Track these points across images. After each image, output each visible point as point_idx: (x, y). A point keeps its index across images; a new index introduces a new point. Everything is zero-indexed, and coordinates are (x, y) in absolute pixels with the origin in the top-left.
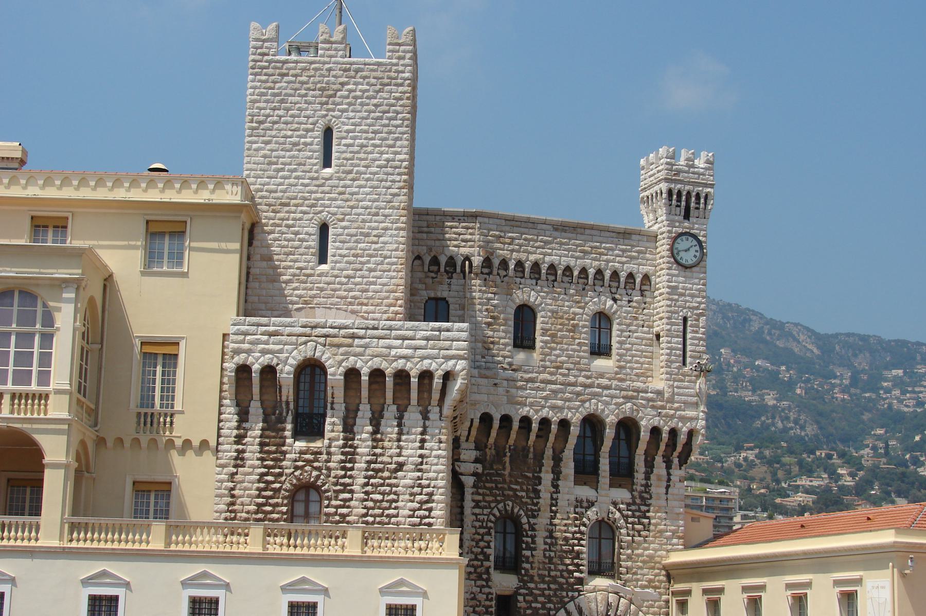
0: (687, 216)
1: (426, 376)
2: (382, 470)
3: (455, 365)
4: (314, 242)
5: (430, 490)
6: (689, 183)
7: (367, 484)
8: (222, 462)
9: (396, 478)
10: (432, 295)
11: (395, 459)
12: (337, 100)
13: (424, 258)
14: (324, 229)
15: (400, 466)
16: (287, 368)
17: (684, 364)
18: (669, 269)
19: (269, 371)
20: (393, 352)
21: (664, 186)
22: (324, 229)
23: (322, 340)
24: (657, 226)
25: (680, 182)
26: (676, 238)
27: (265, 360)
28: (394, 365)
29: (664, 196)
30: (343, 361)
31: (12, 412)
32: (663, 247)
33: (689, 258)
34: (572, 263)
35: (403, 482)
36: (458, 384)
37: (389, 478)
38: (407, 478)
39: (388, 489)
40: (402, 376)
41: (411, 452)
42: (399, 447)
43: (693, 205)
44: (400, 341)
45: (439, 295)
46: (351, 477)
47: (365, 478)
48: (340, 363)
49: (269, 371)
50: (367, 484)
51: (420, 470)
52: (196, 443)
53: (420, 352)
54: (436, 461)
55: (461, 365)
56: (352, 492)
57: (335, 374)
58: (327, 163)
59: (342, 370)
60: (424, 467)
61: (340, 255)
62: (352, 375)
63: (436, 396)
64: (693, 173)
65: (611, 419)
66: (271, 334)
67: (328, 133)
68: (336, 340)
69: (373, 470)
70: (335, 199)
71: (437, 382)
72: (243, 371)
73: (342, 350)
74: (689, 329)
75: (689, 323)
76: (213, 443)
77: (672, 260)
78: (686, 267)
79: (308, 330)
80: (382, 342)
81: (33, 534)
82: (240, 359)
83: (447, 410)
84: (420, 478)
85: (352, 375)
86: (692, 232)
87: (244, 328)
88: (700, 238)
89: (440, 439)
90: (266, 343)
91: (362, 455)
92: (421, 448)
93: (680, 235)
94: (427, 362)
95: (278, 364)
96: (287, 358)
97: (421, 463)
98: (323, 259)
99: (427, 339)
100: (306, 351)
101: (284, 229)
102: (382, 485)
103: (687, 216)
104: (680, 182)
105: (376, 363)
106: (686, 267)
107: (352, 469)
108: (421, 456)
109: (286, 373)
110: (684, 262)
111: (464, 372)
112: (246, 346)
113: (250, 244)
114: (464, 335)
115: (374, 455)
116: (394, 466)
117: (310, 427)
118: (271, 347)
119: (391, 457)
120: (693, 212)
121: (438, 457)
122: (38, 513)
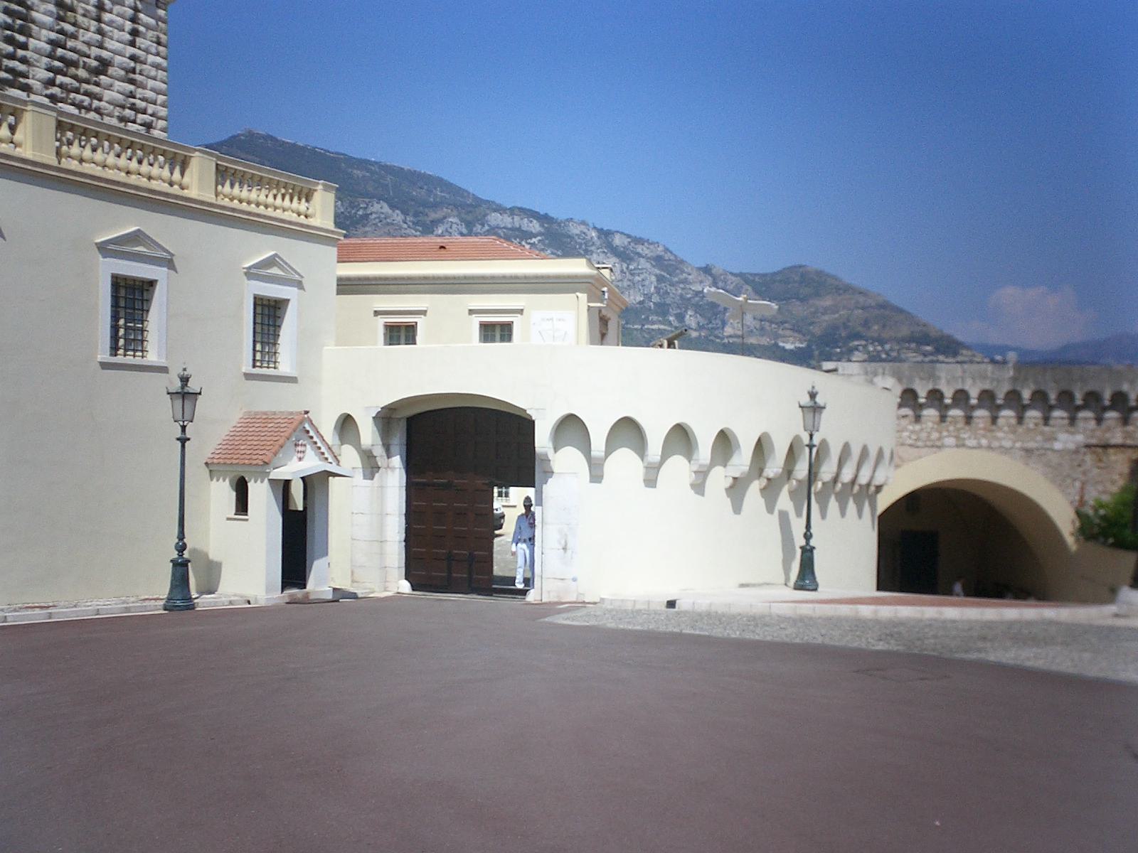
2: (74, 64)
5: (146, 118)
7: (51, 83)
9: (97, 84)
11: (95, 51)
15: (104, 65)
35: (108, 95)
37: (87, 82)
38: (114, 90)
39: (87, 100)
41: (116, 44)
42: (100, 32)
46: (24, 60)
47: (49, 69)
50: (51, 83)
51: (132, 82)
54: (153, 72)
56: (27, 89)
60: (138, 77)
69: (61, 59)
84: (132, 95)
89: (158, 37)
91: (42, 26)
92: (132, 44)
97: (133, 71)
102: (77, 91)
107: (24, 47)
108: (133, 58)
115: (61, 32)
116: (95, 63)
119: (88, 44)
121: (157, 67)
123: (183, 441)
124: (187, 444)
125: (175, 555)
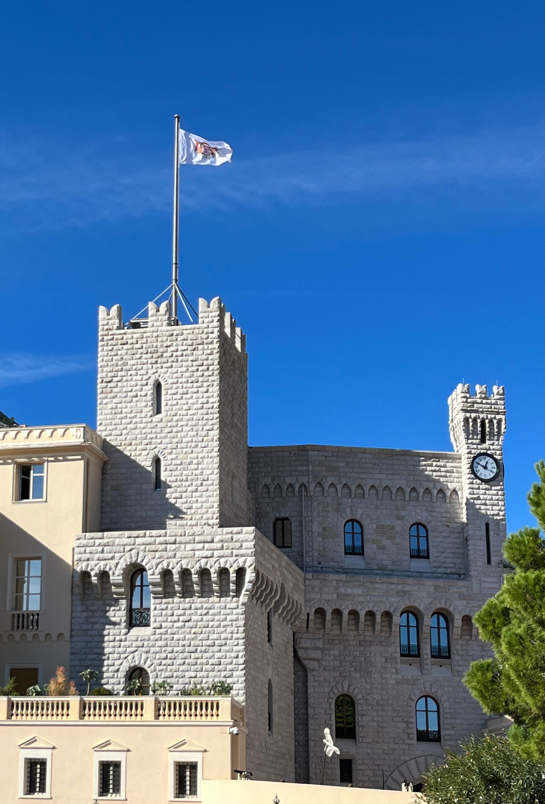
0: (483, 441)
1: (223, 572)
3: (245, 562)
6: (482, 412)
10: (278, 515)
13: (269, 486)
16: (117, 573)
18: (472, 483)
19: (104, 575)
20: (197, 553)
23: (143, 547)
25: (476, 411)
26: (475, 458)
32: (465, 465)
34: (390, 484)
36: (249, 576)
40: (204, 573)
43: (487, 429)
44: (202, 545)
45: (283, 515)
48: (157, 565)
49: (104, 575)
53: (216, 553)
55: (250, 560)
57: (153, 576)
62: (166, 574)
63: (232, 587)
64: (487, 403)
68: (153, 547)
73: (158, 554)
77: (473, 476)
78: (486, 481)
80: (189, 547)
83: (243, 598)
85: (166, 574)
86: (489, 452)
87: (85, 542)
88: (496, 457)
93: (480, 455)
94: (222, 560)
95: (110, 569)
96: (117, 564)
100: (131, 557)
104: (476, 411)
105: (184, 564)
106: (486, 481)
109: (116, 577)
110: (483, 477)
111: (253, 567)
113: (103, 479)
114: (252, 536)
118: (105, 555)
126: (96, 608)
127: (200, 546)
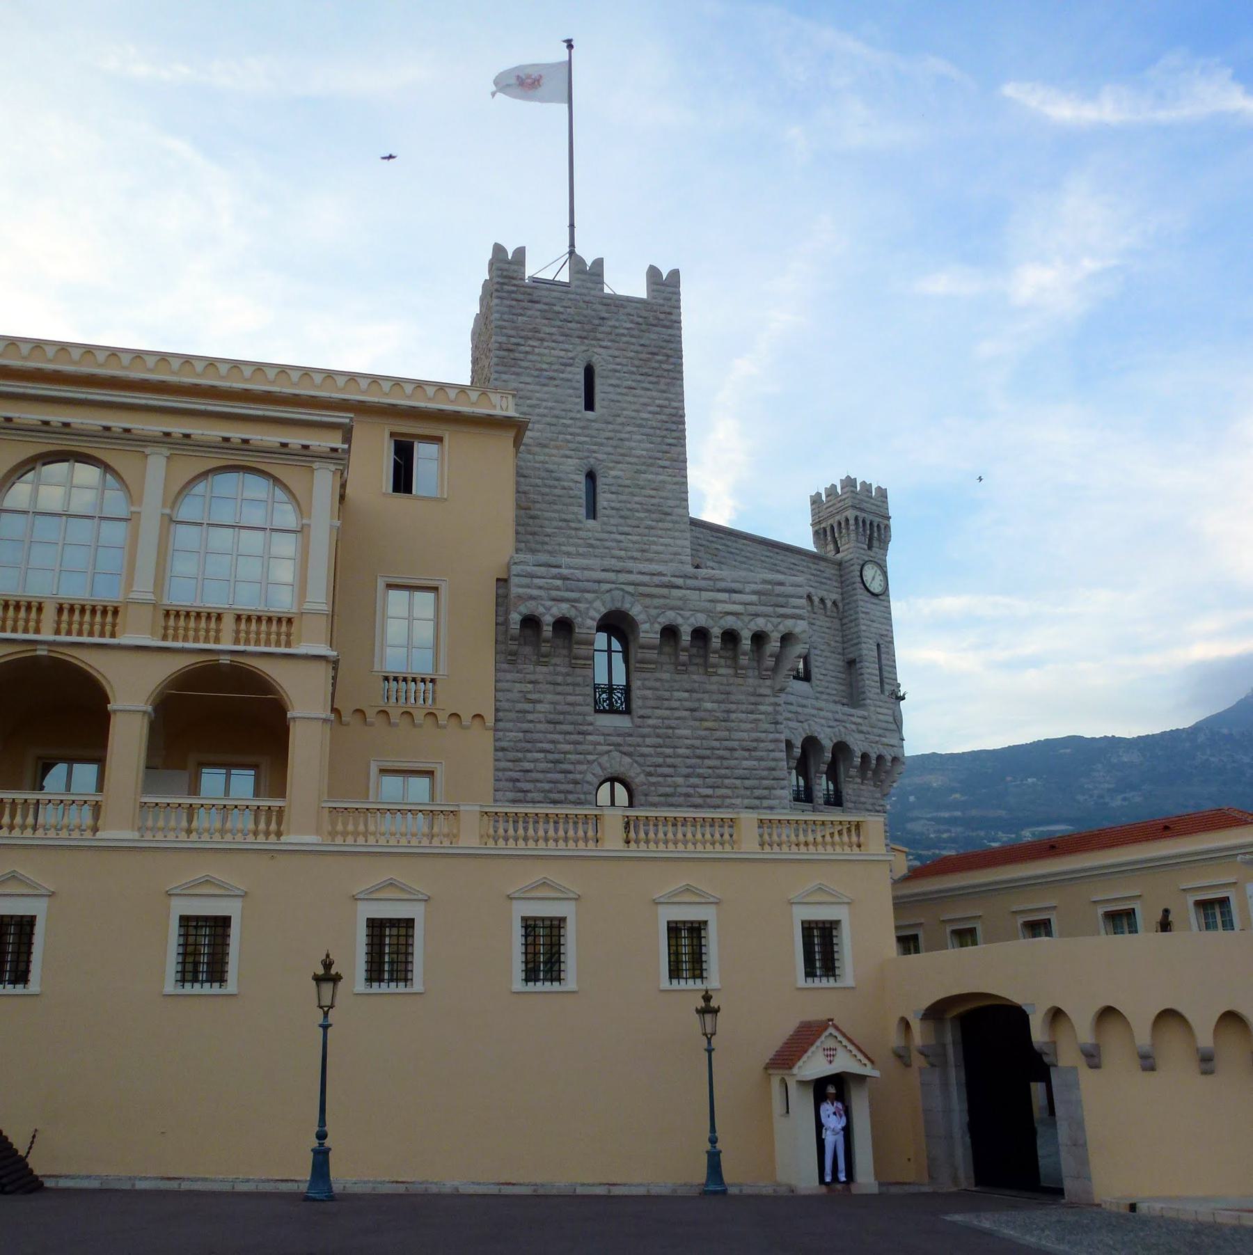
0: (870, 547)
1: (759, 638)
4: (581, 489)
8: (504, 744)
12: (600, 336)
14: (591, 476)
17: (882, 692)
19: (564, 626)
21: (851, 514)
22: (591, 476)
23: (630, 589)
24: (839, 556)
27: (563, 609)
28: (722, 622)
29: (852, 522)
30: (658, 615)
31: (237, 641)
33: (876, 587)
40: (731, 637)
44: (726, 595)
49: (564, 626)
52: (466, 718)
57: (648, 632)
58: (589, 405)
59: (658, 628)
61: (613, 508)
62: (670, 633)
63: (770, 662)
65: (828, 744)
66: (565, 578)
67: (589, 373)
70: (601, 445)
71: (774, 645)
72: (531, 622)
73: (657, 602)
74: (883, 656)
75: (883, 650)
76: (490, 721)
78: (873, 594)
79: (611, 576)
80: (705, 595)
81: (273, 827)
82: (525, 609)
85: (670, 633)
90: (558, 589)
98: (592, 512)
99: (754, 593)
101: (544, 474)
103: (870, 547)
105: (701, 620)
112: (535, 592)
117: (616, 701)
120: (875, 543)
122: (281, 793)
123: (710, 1051)
124: (713, 1054)
125: (708, 1146)
126: (540, 677)
127: (724, 596)
